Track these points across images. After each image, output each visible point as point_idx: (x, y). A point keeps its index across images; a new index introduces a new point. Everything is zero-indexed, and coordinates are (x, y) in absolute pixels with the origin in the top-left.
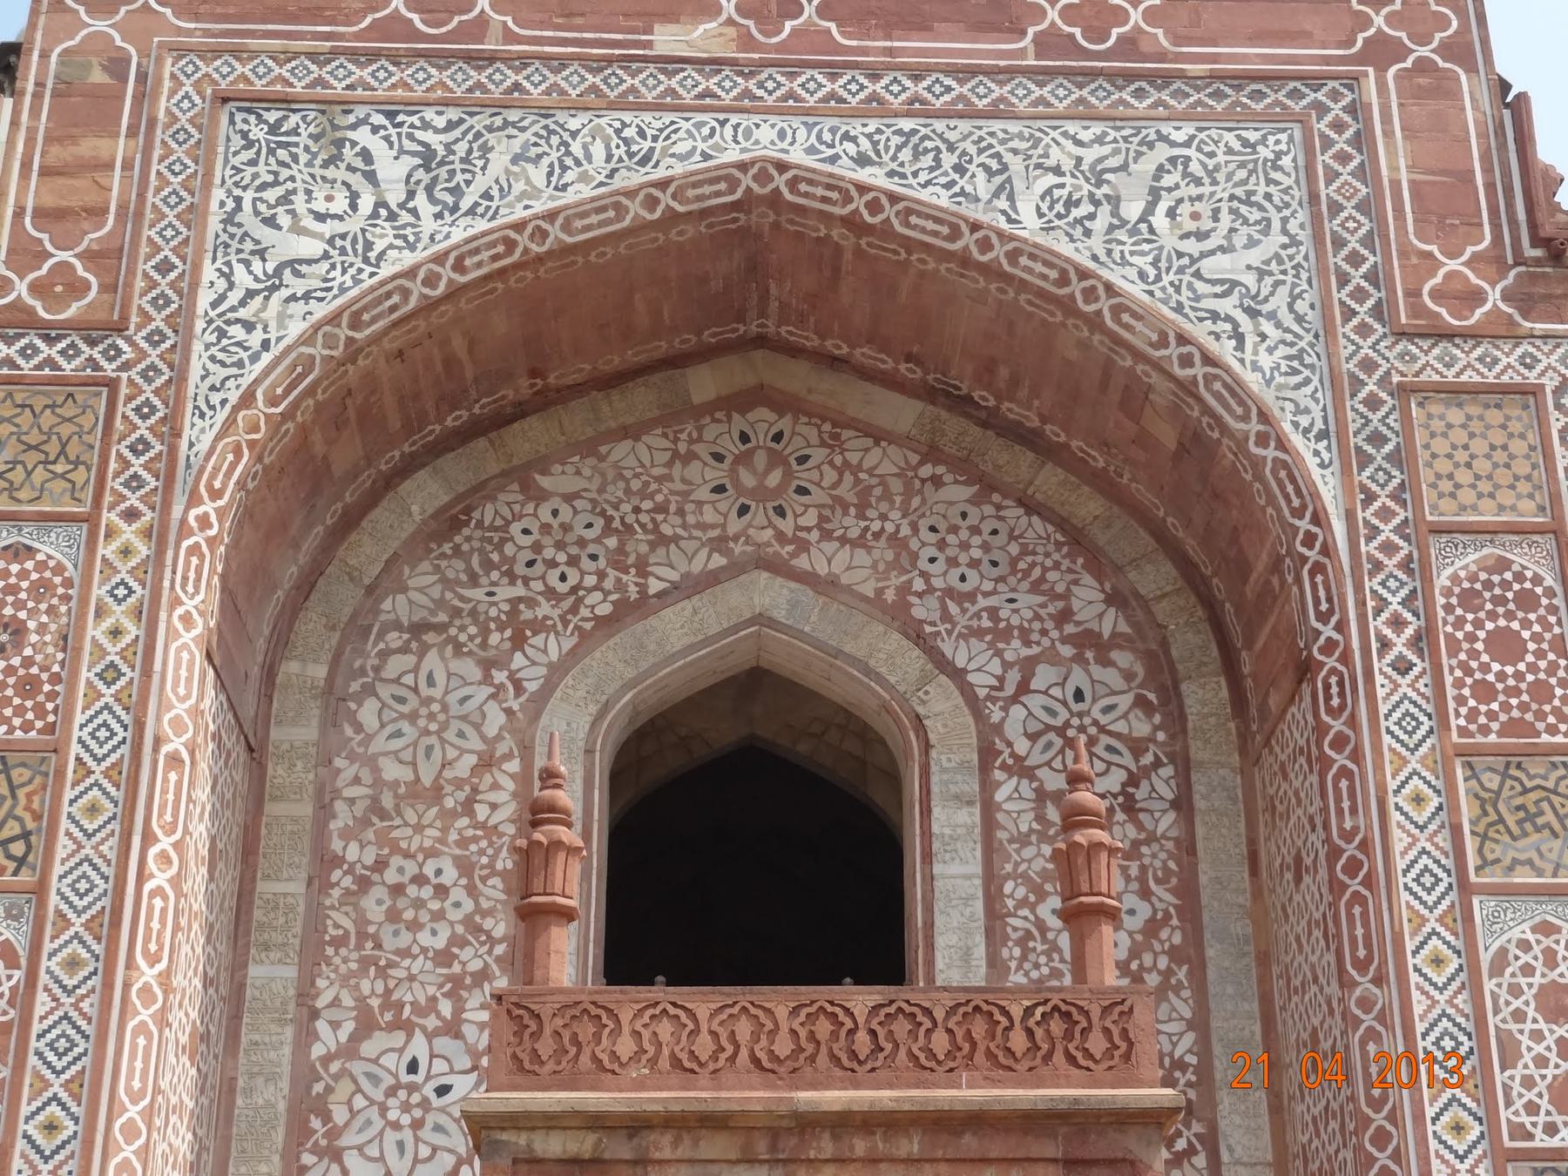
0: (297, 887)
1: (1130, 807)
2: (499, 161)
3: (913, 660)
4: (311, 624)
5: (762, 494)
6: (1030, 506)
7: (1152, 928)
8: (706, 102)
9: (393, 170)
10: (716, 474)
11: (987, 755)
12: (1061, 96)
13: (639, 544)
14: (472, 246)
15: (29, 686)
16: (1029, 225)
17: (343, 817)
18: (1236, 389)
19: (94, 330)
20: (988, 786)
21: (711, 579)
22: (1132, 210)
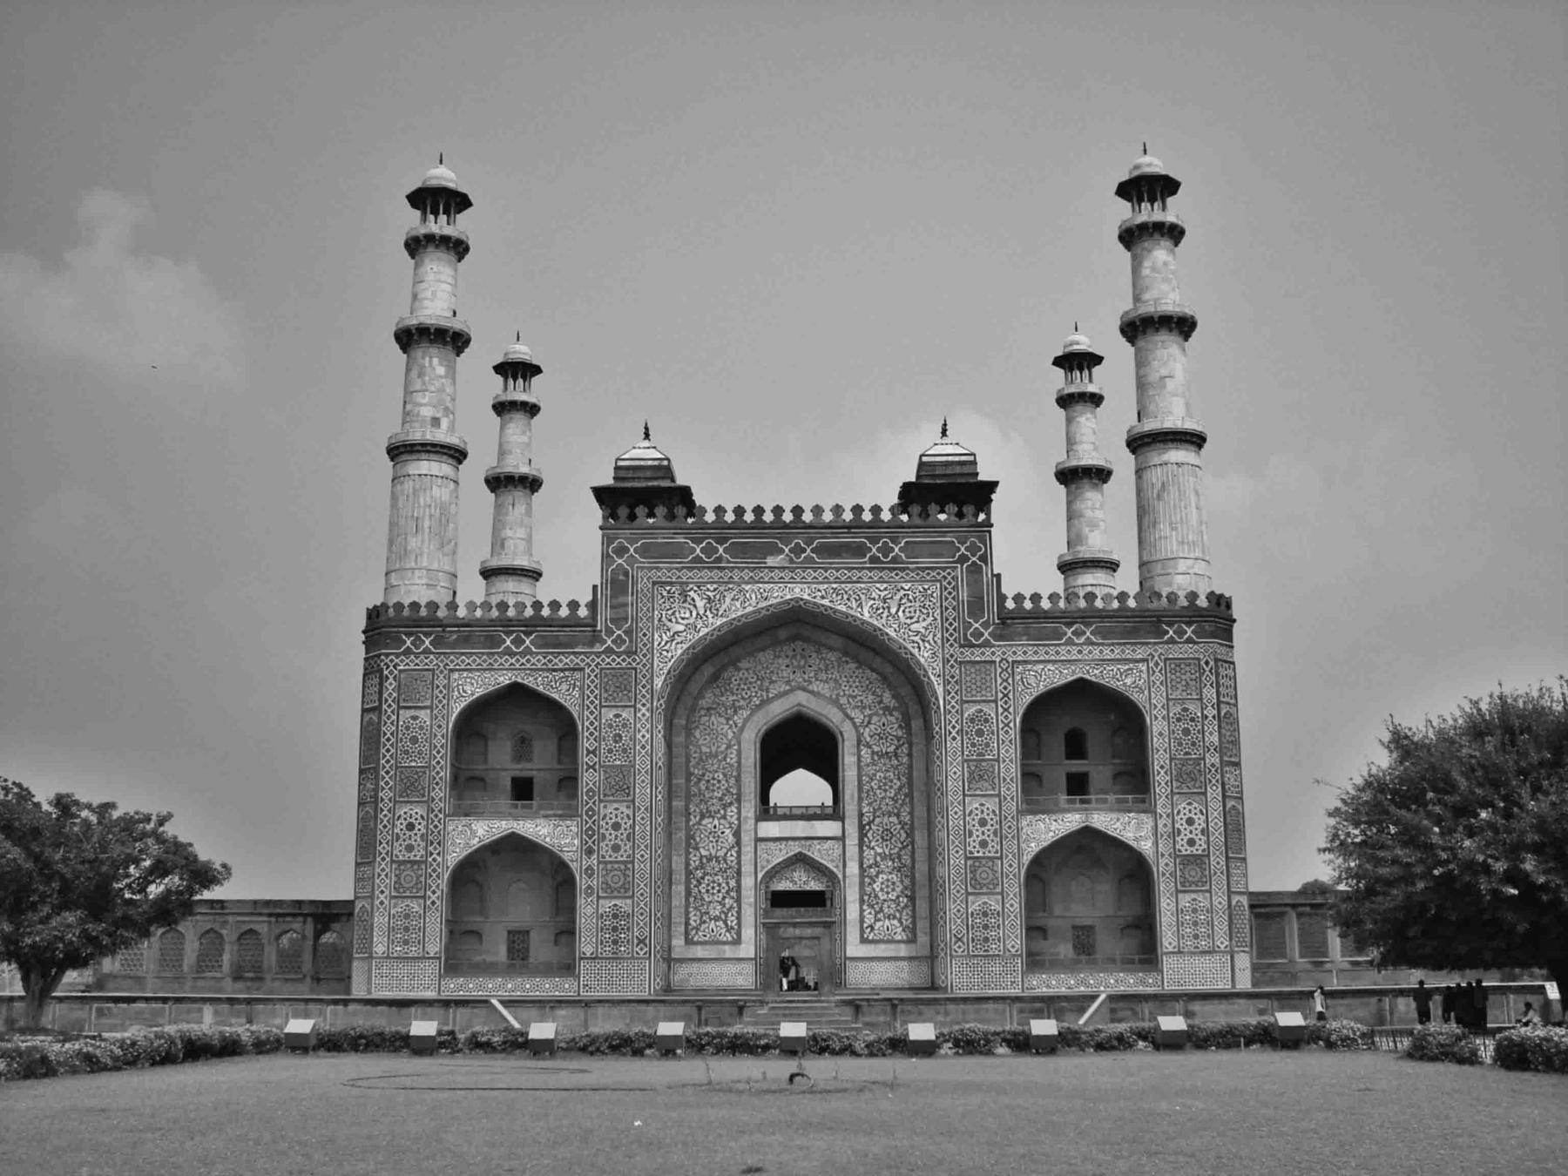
0: (683, 781)
1: (896, 755)
2: (728, 600)
3: (840, 714)
4: (681, 710)
5: (799, 667)
6: (873, 670)
7: (900, 789)
8: (781, 580)
9: (700, 603)
10: (787, 661)
11: (859, 742)
12: (876, 575)
13: (766, 683)
14: (722, 625)
15: (625, 751)
16: (866, 616)
17: (693, 762)
18: (918, 662)
19: (629, 653)
20: (859, 751)
21: (786, 693)
22: (893, 611)
